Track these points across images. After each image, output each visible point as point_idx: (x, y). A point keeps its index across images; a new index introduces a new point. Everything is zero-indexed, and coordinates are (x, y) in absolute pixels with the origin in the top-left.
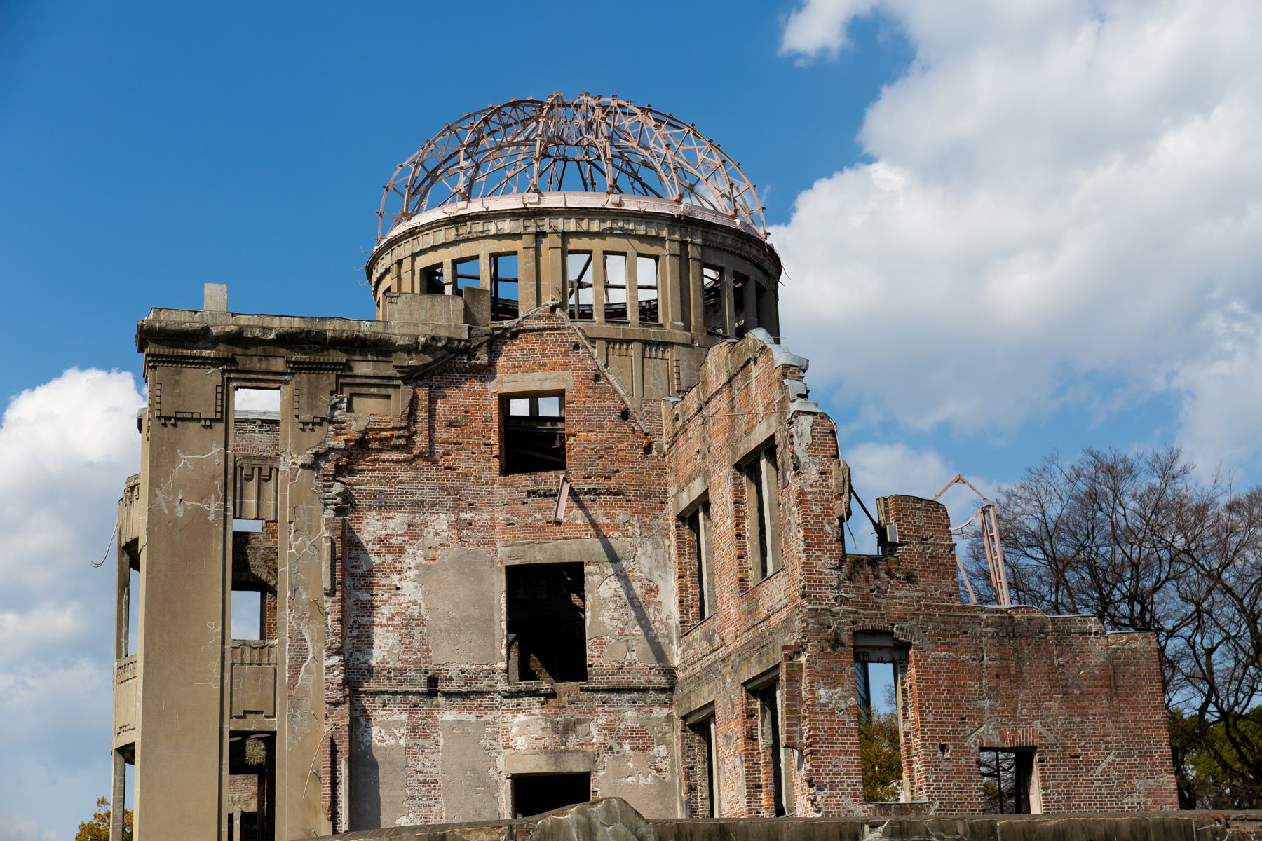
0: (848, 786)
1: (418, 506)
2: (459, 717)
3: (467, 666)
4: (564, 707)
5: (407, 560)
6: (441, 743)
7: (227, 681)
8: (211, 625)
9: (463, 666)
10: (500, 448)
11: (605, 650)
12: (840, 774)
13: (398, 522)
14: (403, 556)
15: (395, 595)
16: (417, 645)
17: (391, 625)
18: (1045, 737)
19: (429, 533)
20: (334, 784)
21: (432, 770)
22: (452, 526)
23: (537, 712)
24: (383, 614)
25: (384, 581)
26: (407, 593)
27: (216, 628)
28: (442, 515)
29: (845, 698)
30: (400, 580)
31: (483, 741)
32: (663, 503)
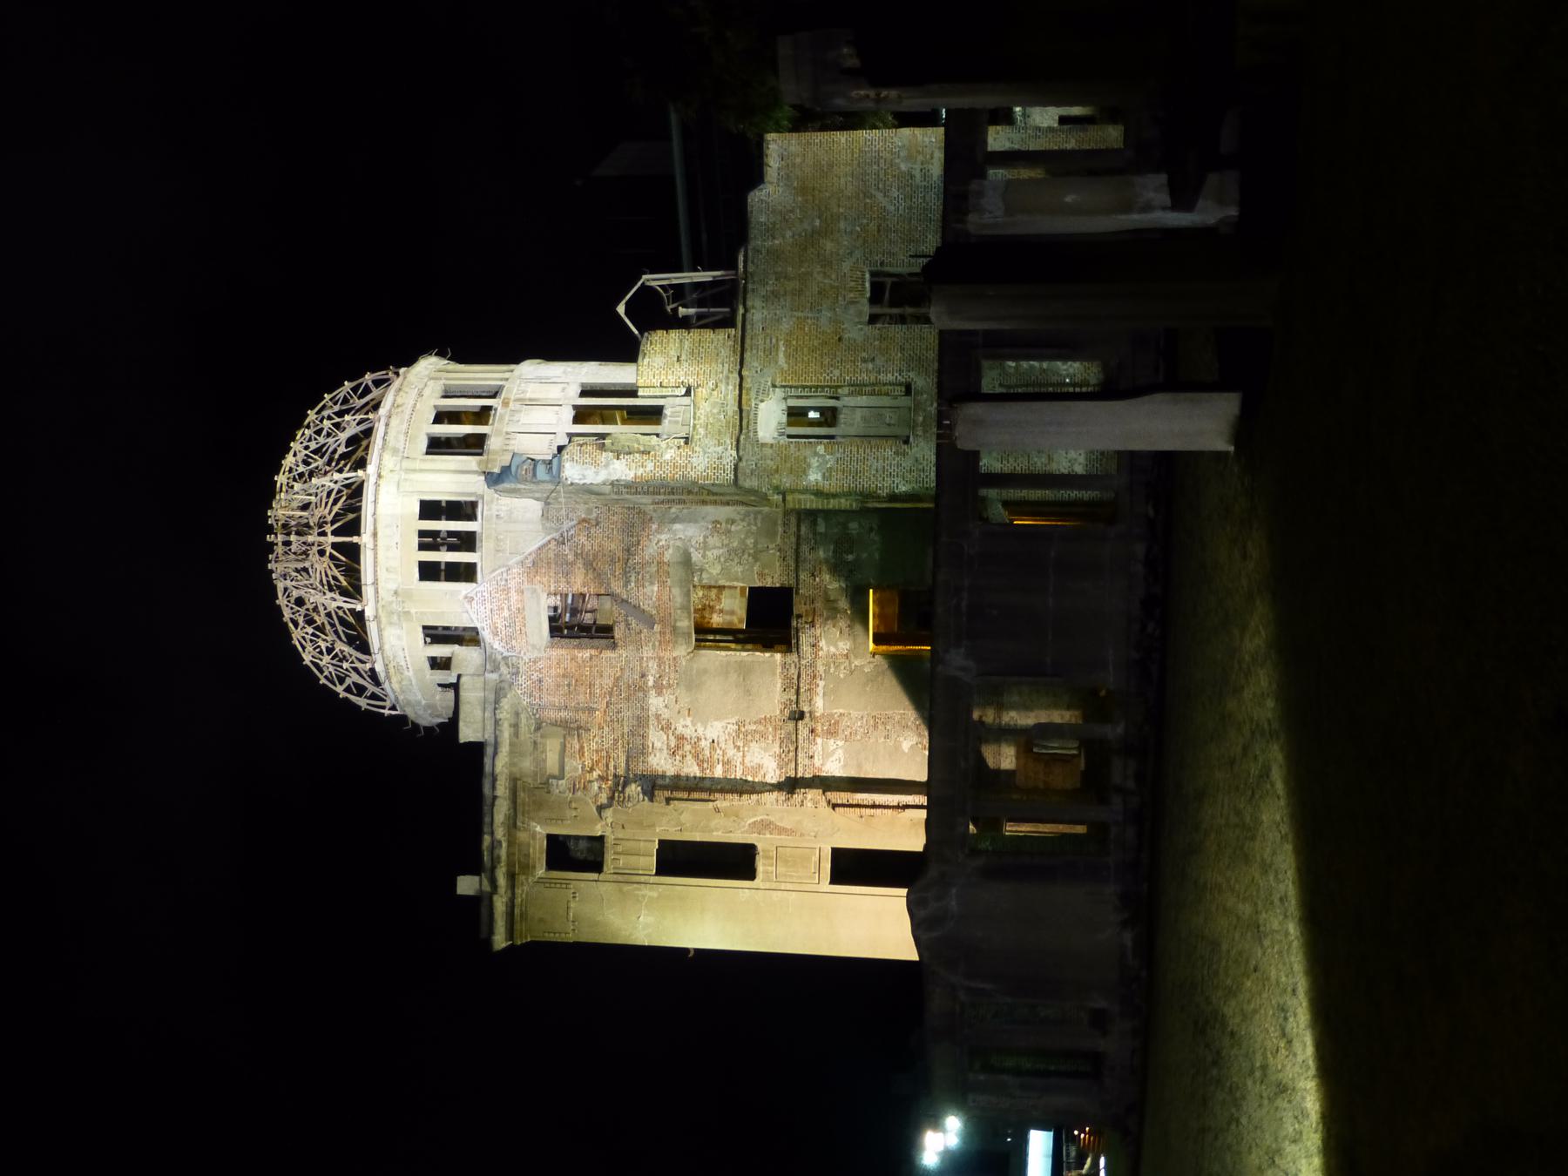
0: (894, 459)
1: (641, 722)
2: (821, 695)
3: (779, 685)
4: (814, 609)
5: (688, 732)
6: (841, 711)
7: (790, 887)
8: (743, 897)
9: (778, 689)
10: (592, 647)
11: (766, 571)
12: (884, 467)
13: (656, 738)
14: (685, 736)
15: (718, 744)
16: (761, 728)
17: (744, 747)
18: (858, 260)
19: (666, 714)
20: (874, 806)
21: (865, 720)
22: (659, 694)
23: (818, 631)
24: (734, 755)
25: (707, 752)
26: (717, 734)
27: (745, 893)
28: (651, 701)
29: (816, 454)
30: (705, 739)
31: (842, 676)
32: (638, 513)
